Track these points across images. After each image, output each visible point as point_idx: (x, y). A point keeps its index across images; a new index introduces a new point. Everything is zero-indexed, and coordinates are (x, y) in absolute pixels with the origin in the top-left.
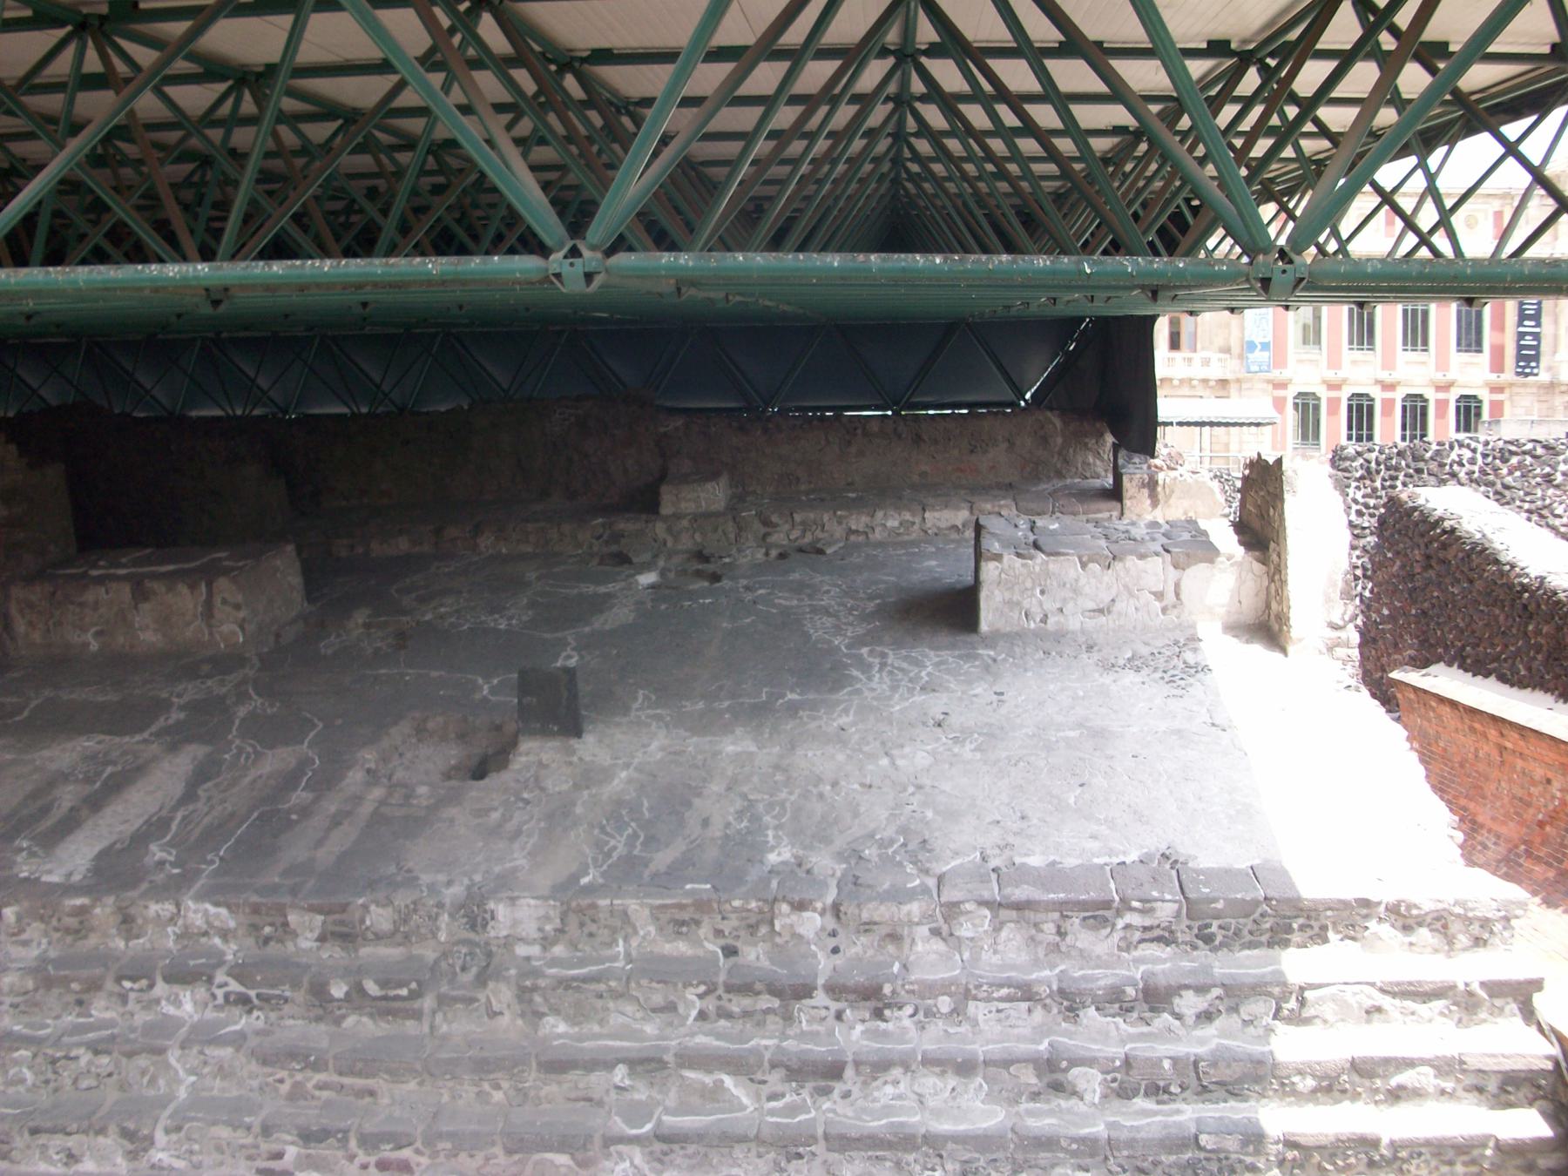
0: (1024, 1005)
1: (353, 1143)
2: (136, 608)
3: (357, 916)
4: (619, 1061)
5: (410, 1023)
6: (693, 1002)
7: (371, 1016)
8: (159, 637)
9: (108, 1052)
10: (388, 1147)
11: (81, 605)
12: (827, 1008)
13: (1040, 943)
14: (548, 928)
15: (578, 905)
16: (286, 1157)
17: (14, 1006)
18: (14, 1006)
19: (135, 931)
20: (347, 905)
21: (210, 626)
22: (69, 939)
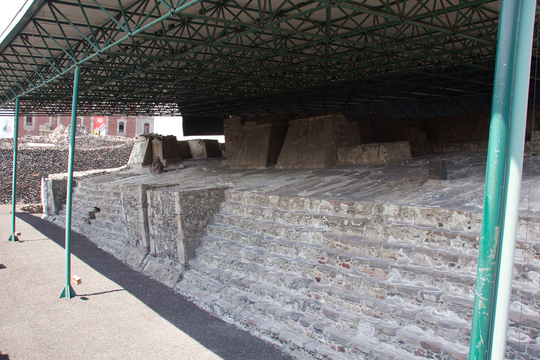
0: (521, 250)
1: (338, 258)
4: (401, 248)
5: (360, 233)
6: (425, 236)
7: (353, 231)
9: (298, 231)
10: (345, 260)
12: (460, 242)
13: (534, 233)
14: (396, 213)
16: (325, 259)
17: (287, 221)
18: (287, 221)
20: (354, 203)
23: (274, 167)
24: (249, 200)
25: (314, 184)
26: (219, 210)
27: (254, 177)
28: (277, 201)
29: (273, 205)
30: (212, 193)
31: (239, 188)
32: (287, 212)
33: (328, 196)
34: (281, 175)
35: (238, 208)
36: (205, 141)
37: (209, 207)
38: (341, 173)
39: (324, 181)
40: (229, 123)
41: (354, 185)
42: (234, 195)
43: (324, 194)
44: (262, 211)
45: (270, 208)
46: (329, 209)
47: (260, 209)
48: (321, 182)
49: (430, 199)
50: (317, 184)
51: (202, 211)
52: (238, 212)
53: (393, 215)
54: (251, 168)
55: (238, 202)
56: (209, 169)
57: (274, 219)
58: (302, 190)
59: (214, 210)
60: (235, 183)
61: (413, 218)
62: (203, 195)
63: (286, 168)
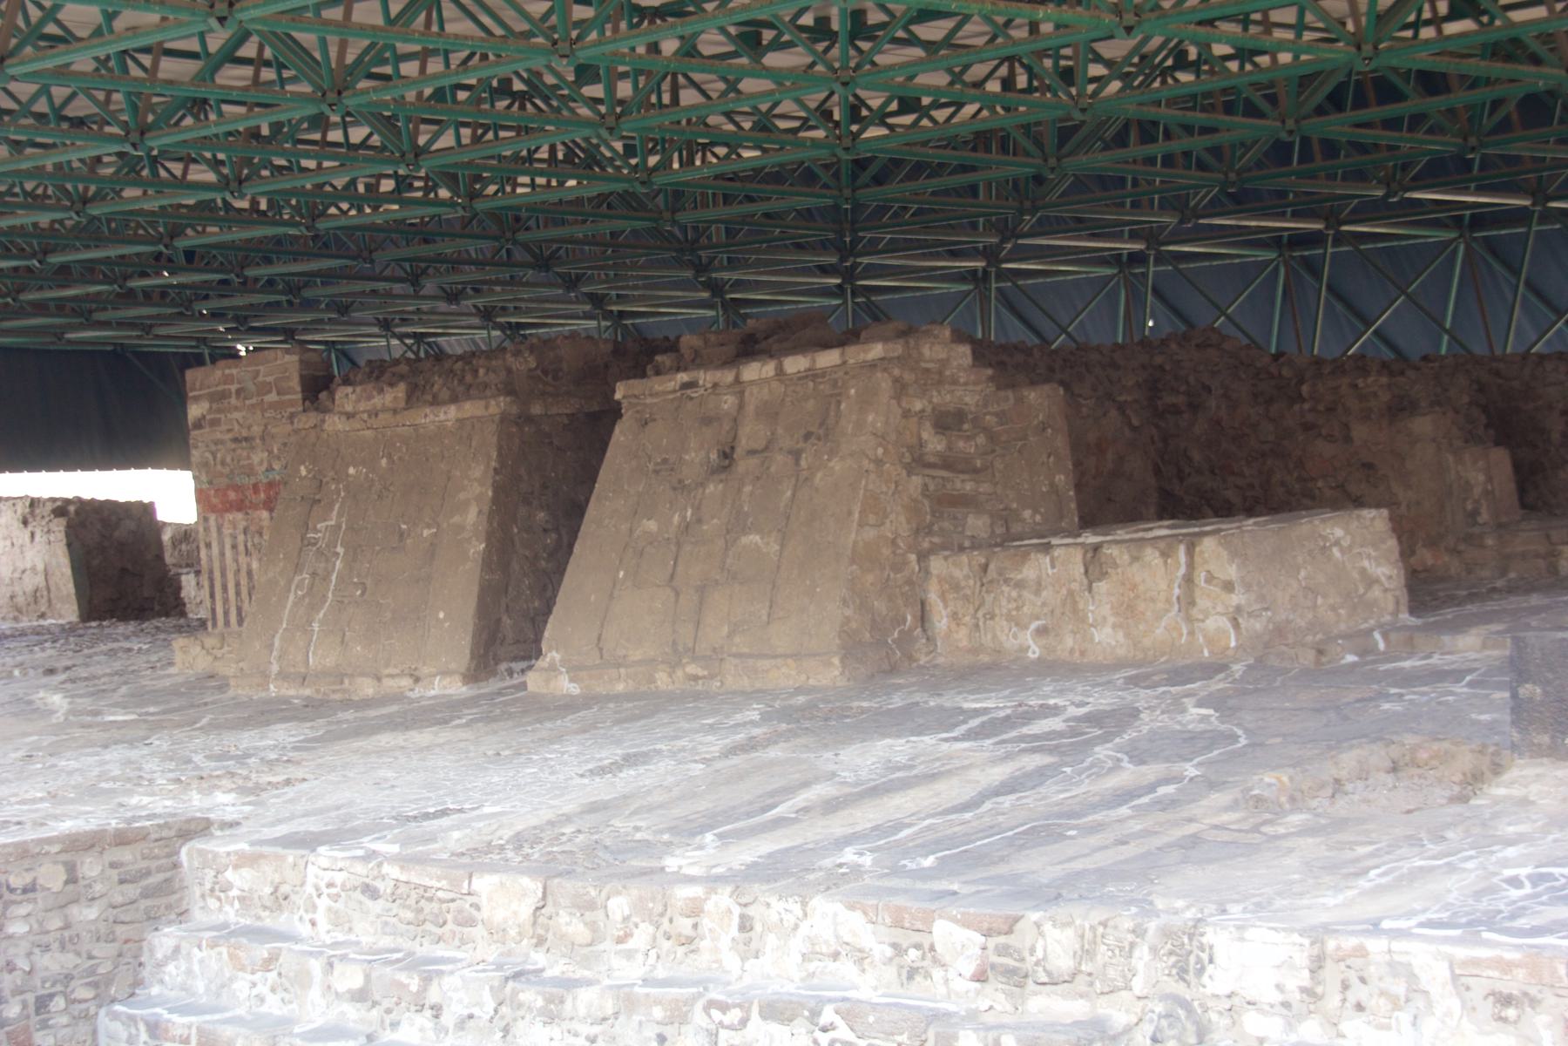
2: (1090, 589)
3: (1028, 944)
8: (1120, 636)
11: (1020, 585)
15: (1339, 948)
19: (754, 945)
20: (1017, 920)
21: (1189, 619)
22: (681, 950)
23: (523, 686)
24: (339, 905)
25: (772, 794)
26: (138, 983)
27: (380, 752)
28: (525, 910)
29: (497, 933)
30: (90, 867)
31: (282, 830)
32: (589, 983)
33: (857, 870)
34: (559, 738)
35: (268, 963)
36: (66, 510)
37: (69, 960)
38: (946, 720)
39: (834, 774)
40: (224, 396)
41: (1030, 798)
42: (246, 872)
43: (828, 862)
44: (427, 980)
45: (479, 956)
46: (861, 957)
47: (412, 963)
48: (817, 780)
49: (1515, 893)
50: (789, 791)
51: (18, 991)
52: (263, 989)
53: (1277, 997)
54: (367, 688)
55: (268, 921)
56: (85, 703)
57: (506, 1031)
58: (688, 831)
59: (101, 987)
60: (254, 791)
61: (1404, 1017)
62: (28, 878)
63: (601, 689)
